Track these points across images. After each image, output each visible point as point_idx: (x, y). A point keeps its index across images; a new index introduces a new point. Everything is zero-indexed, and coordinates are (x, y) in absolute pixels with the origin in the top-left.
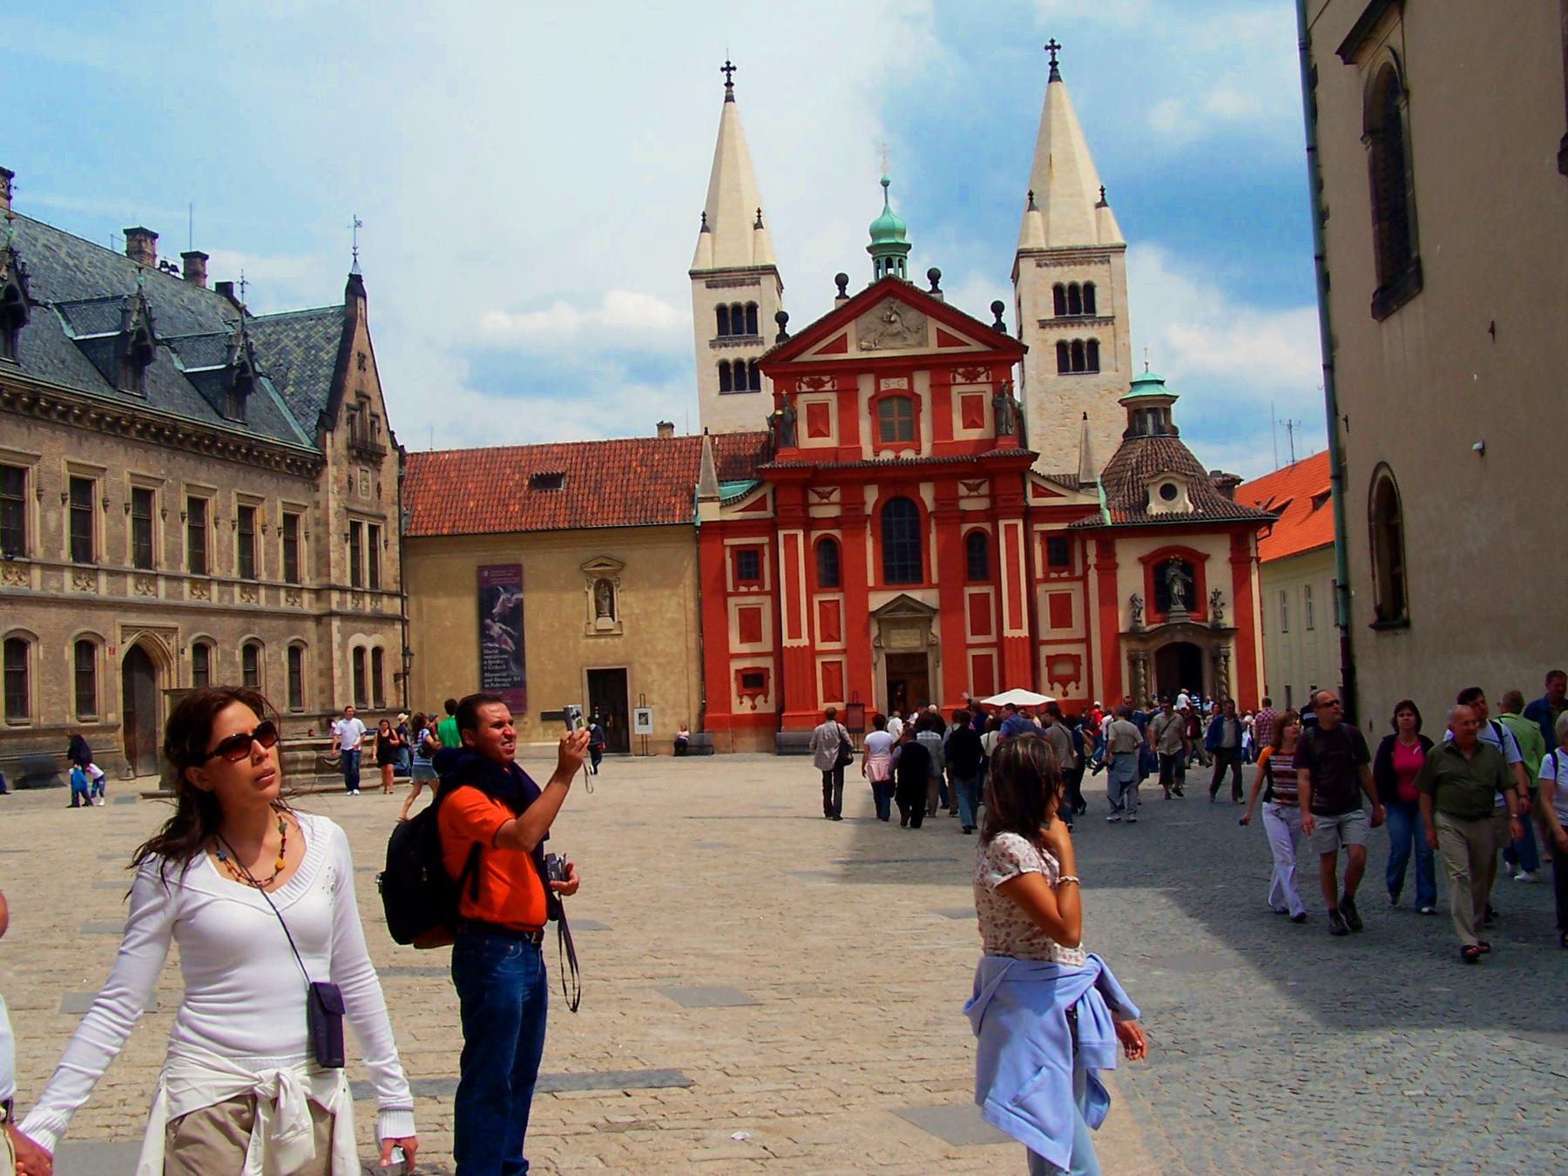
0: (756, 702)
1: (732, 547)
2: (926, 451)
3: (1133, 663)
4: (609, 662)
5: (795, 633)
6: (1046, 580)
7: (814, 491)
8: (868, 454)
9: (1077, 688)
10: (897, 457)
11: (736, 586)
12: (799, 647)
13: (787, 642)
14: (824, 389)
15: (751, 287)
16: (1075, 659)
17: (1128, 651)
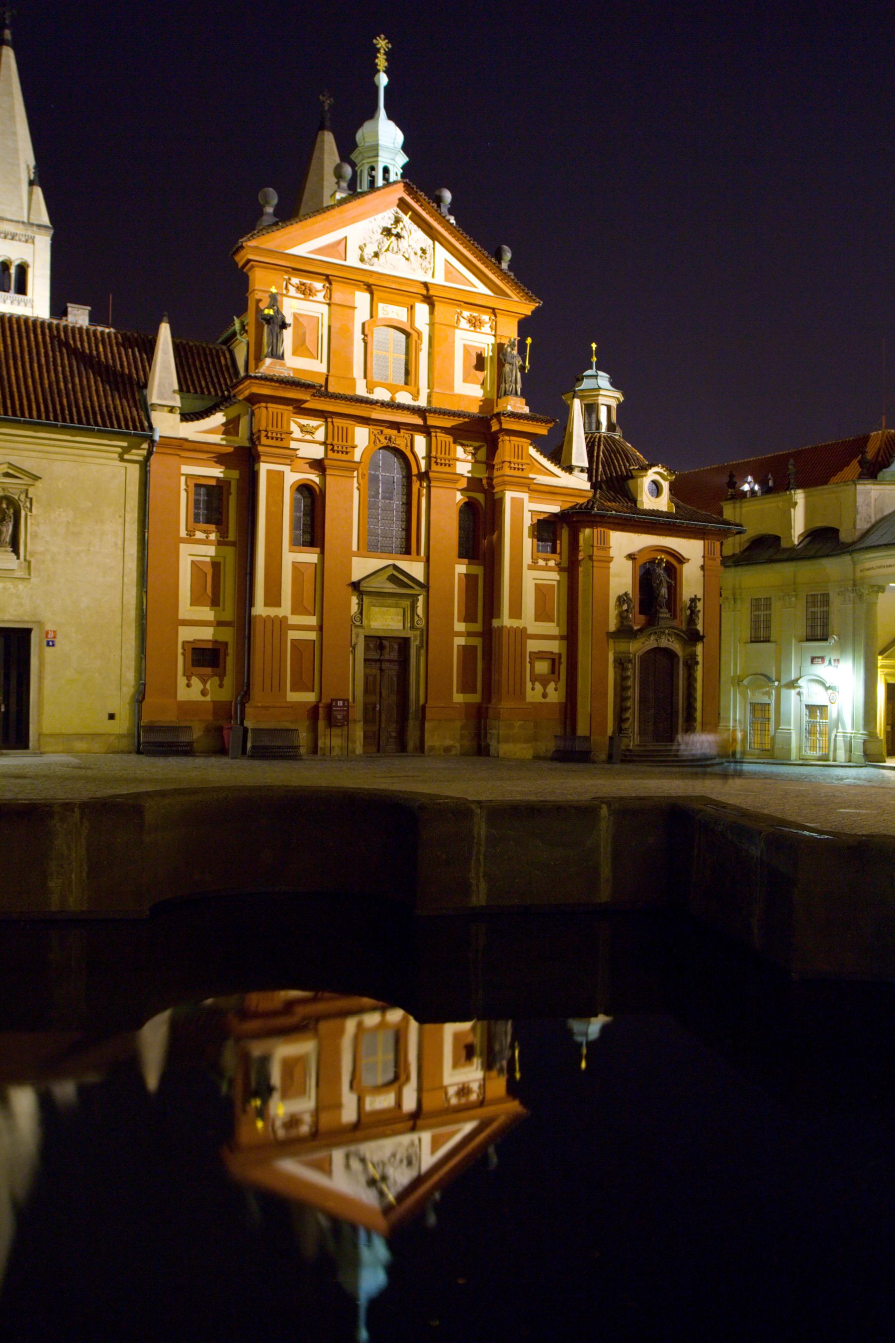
0: (208, 686)
1: (188, 476)
2: (422, 402)
3: (621, 663)
4: (7, 617)
5: (273, 599)
6: (534, 566)
7: (296, 422)
8: (361, 390)
9: (556, 690)
10: (392, 399)
11: (191, 533)
12: (276, 616)
13: (260, 609)
14: (315, 298)
15: (23, 245)
16: (554, 660)
17: (615, 653)
